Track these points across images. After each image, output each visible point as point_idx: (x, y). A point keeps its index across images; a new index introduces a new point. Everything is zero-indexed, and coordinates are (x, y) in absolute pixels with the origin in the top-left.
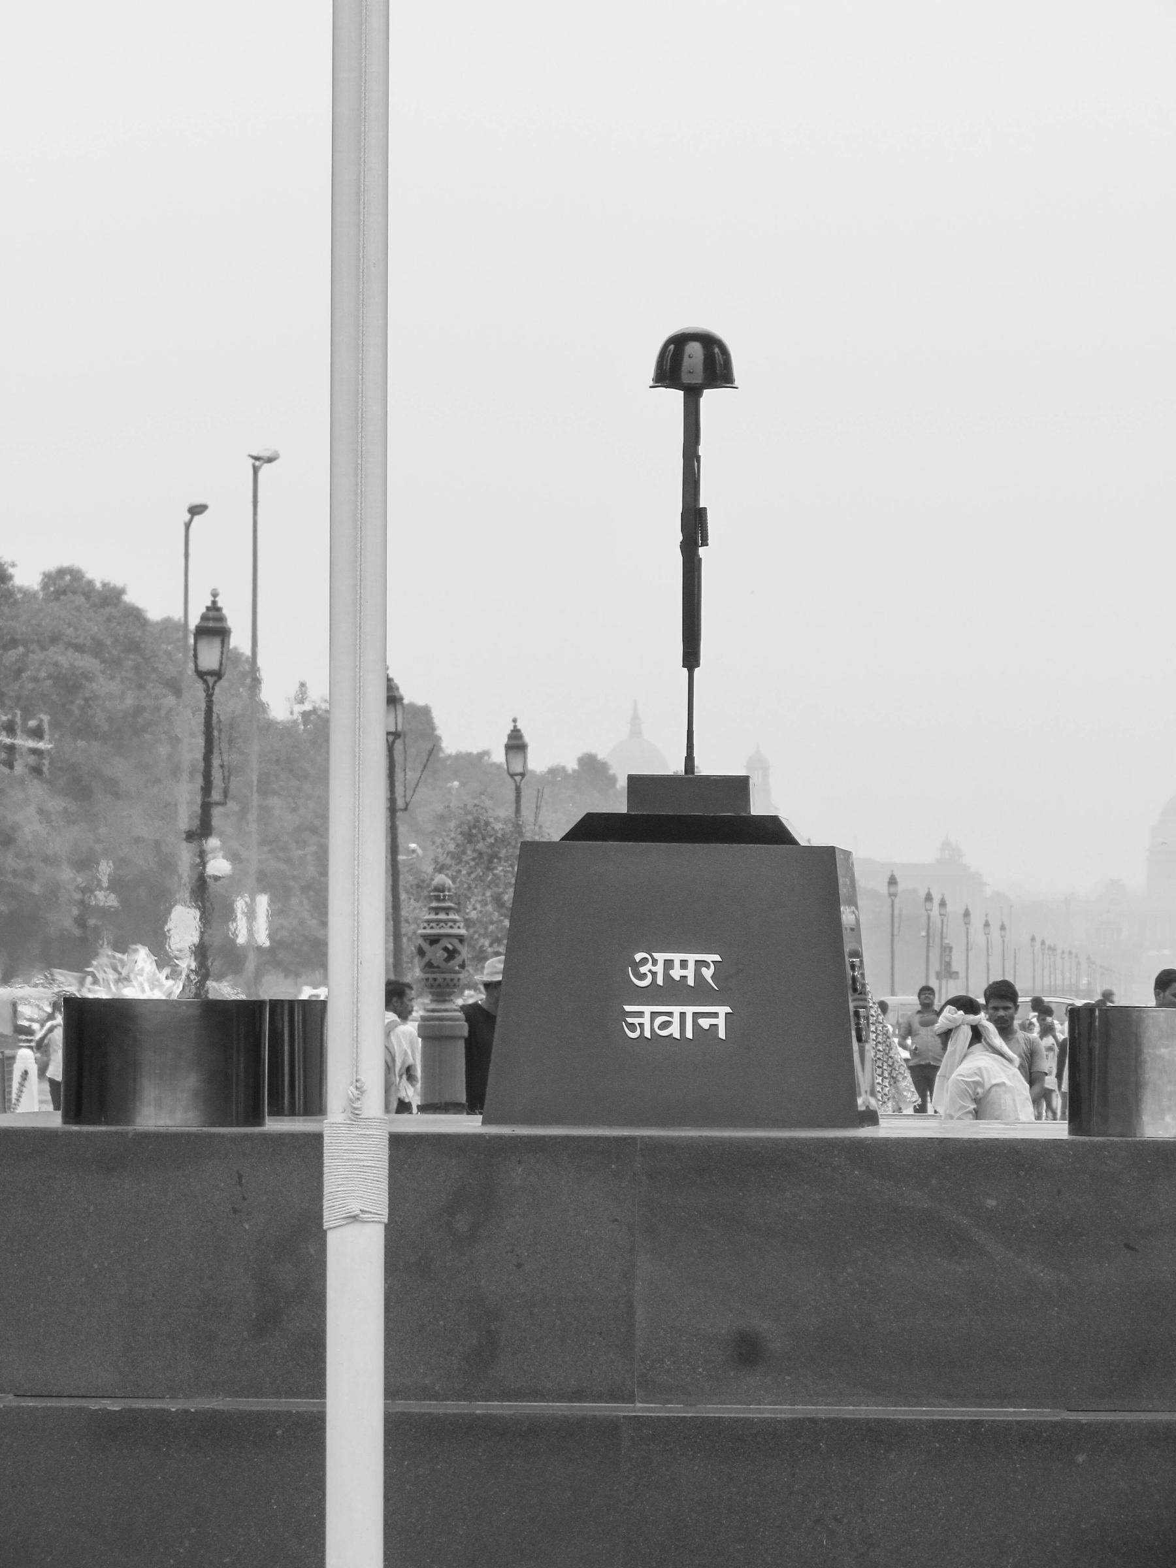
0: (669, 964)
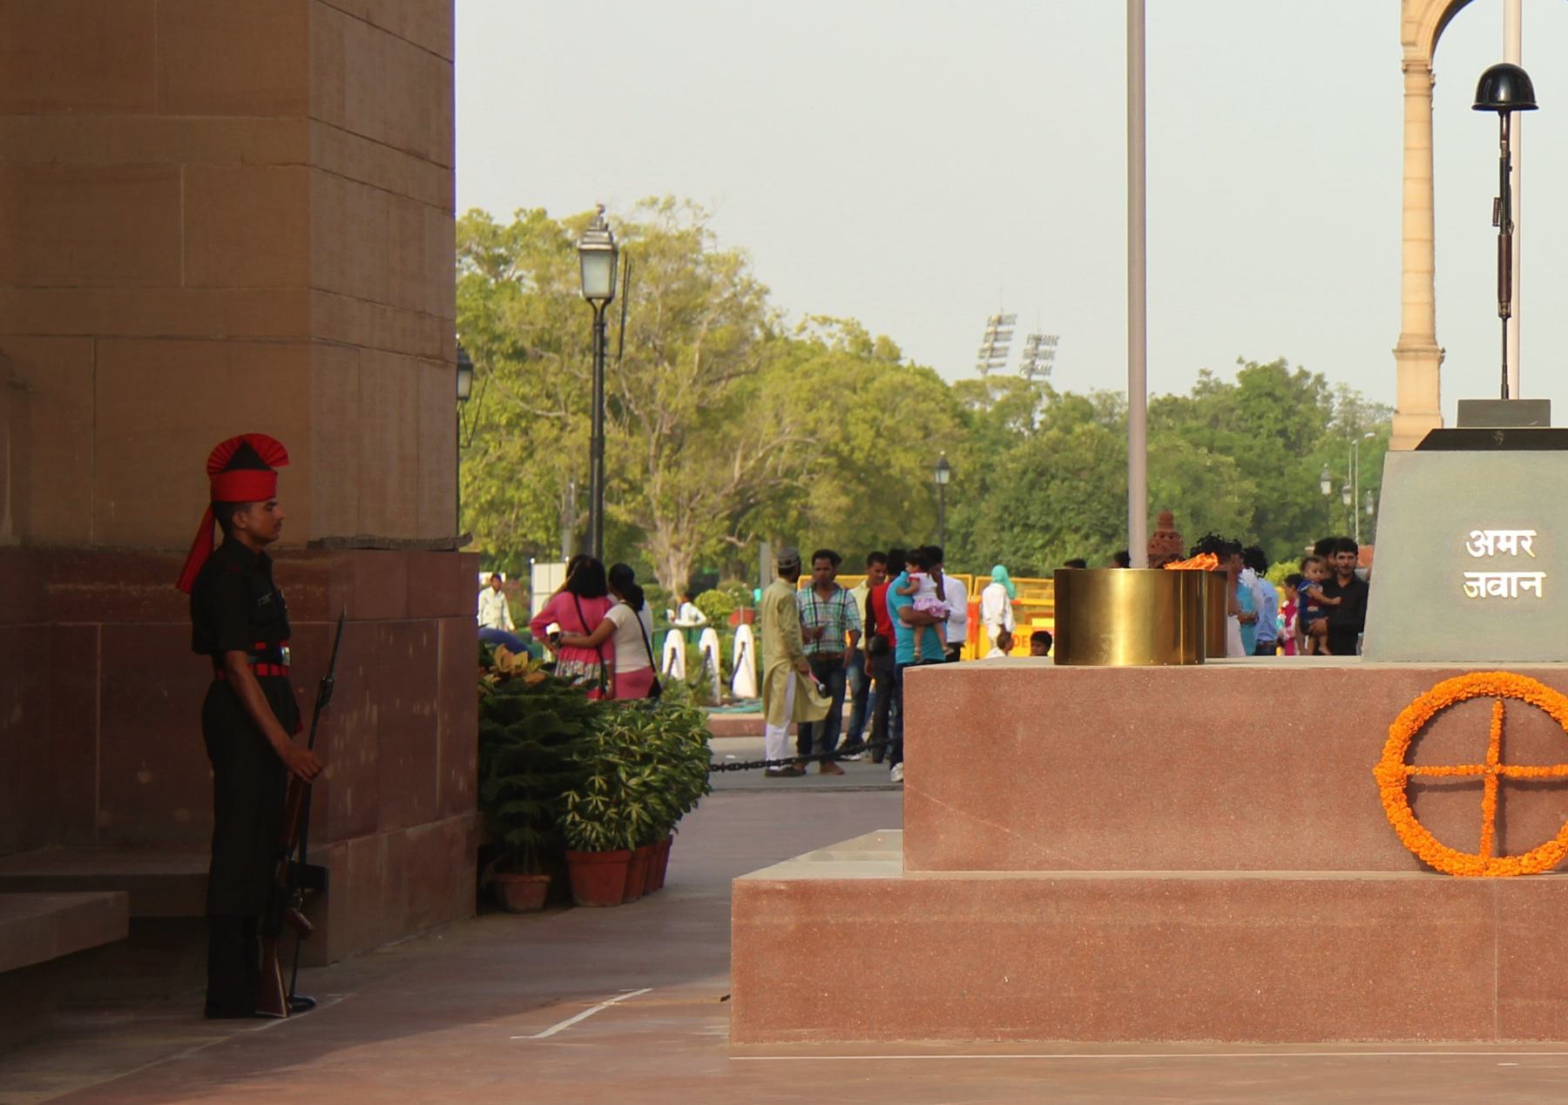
0: (1497, 539)
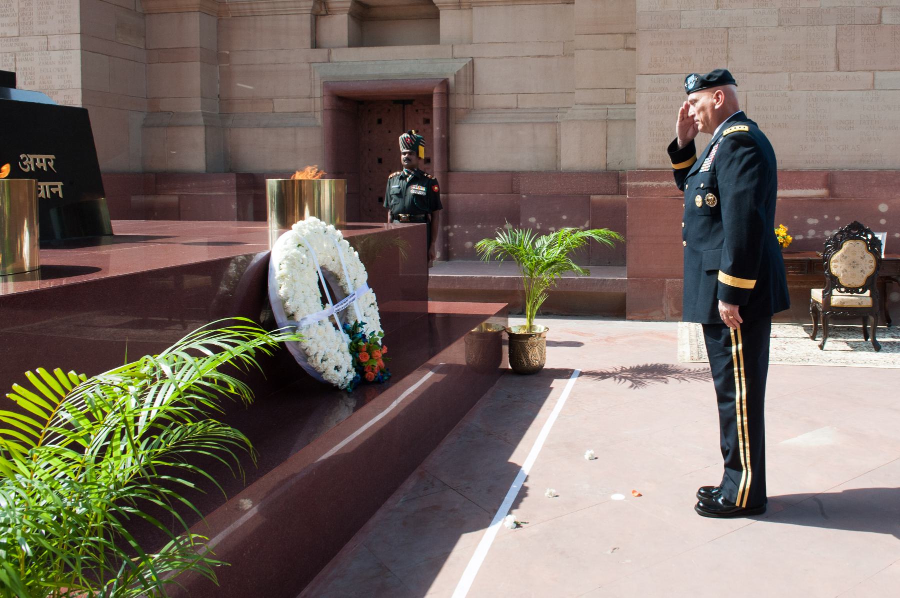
0: (35, 160)
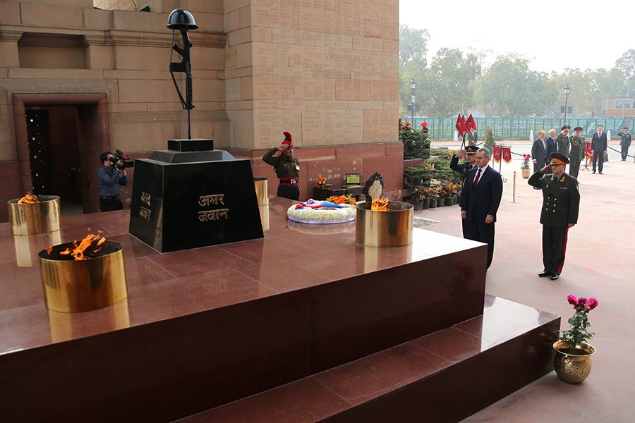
0: (210, 199)
